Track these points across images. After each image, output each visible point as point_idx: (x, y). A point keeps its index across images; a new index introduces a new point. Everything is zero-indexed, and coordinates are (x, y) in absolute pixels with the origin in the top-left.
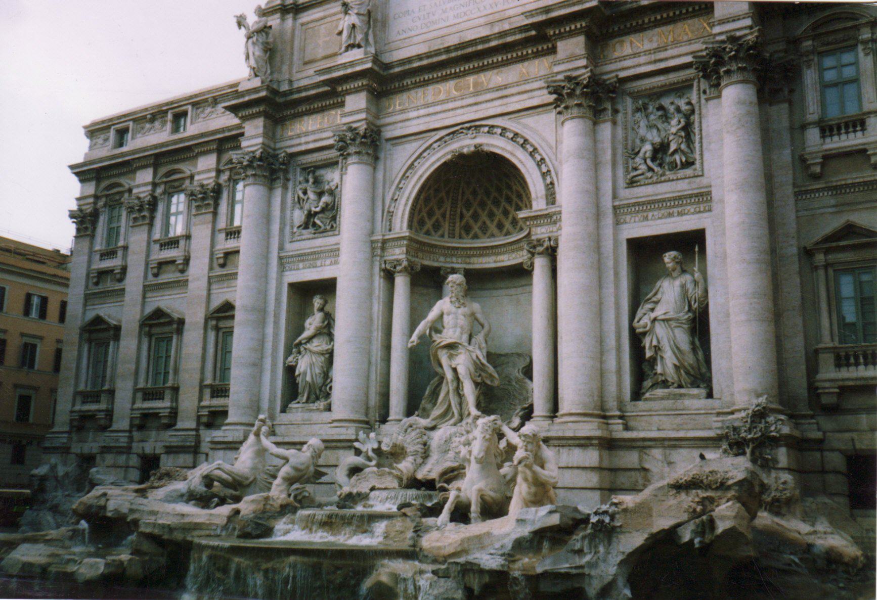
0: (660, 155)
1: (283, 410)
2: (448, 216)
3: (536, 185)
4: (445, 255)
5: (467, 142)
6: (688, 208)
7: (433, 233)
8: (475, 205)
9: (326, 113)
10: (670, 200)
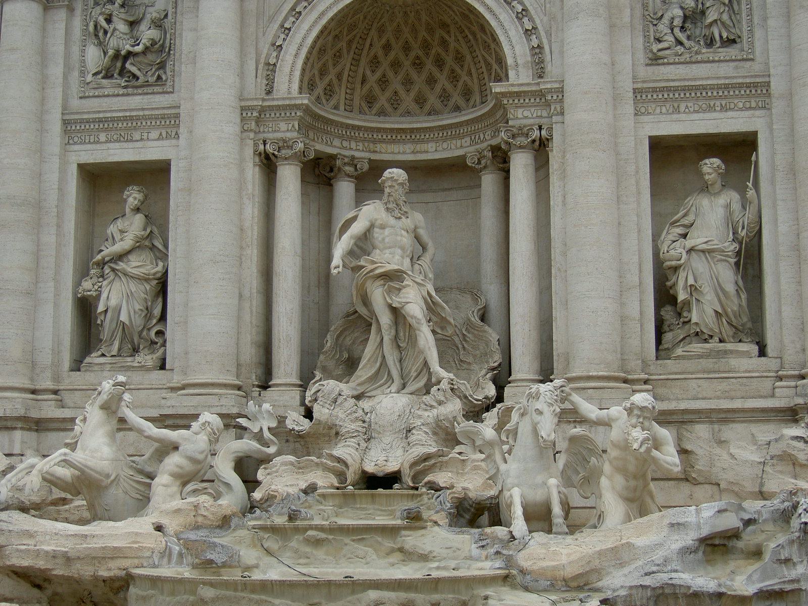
0: (688, 25)
1: (77, 365)
3: (514, 47)
4: (342, 137)
6: (736, 102)
7: (324, 101)
8: (385, 65)
10: (712, 87)
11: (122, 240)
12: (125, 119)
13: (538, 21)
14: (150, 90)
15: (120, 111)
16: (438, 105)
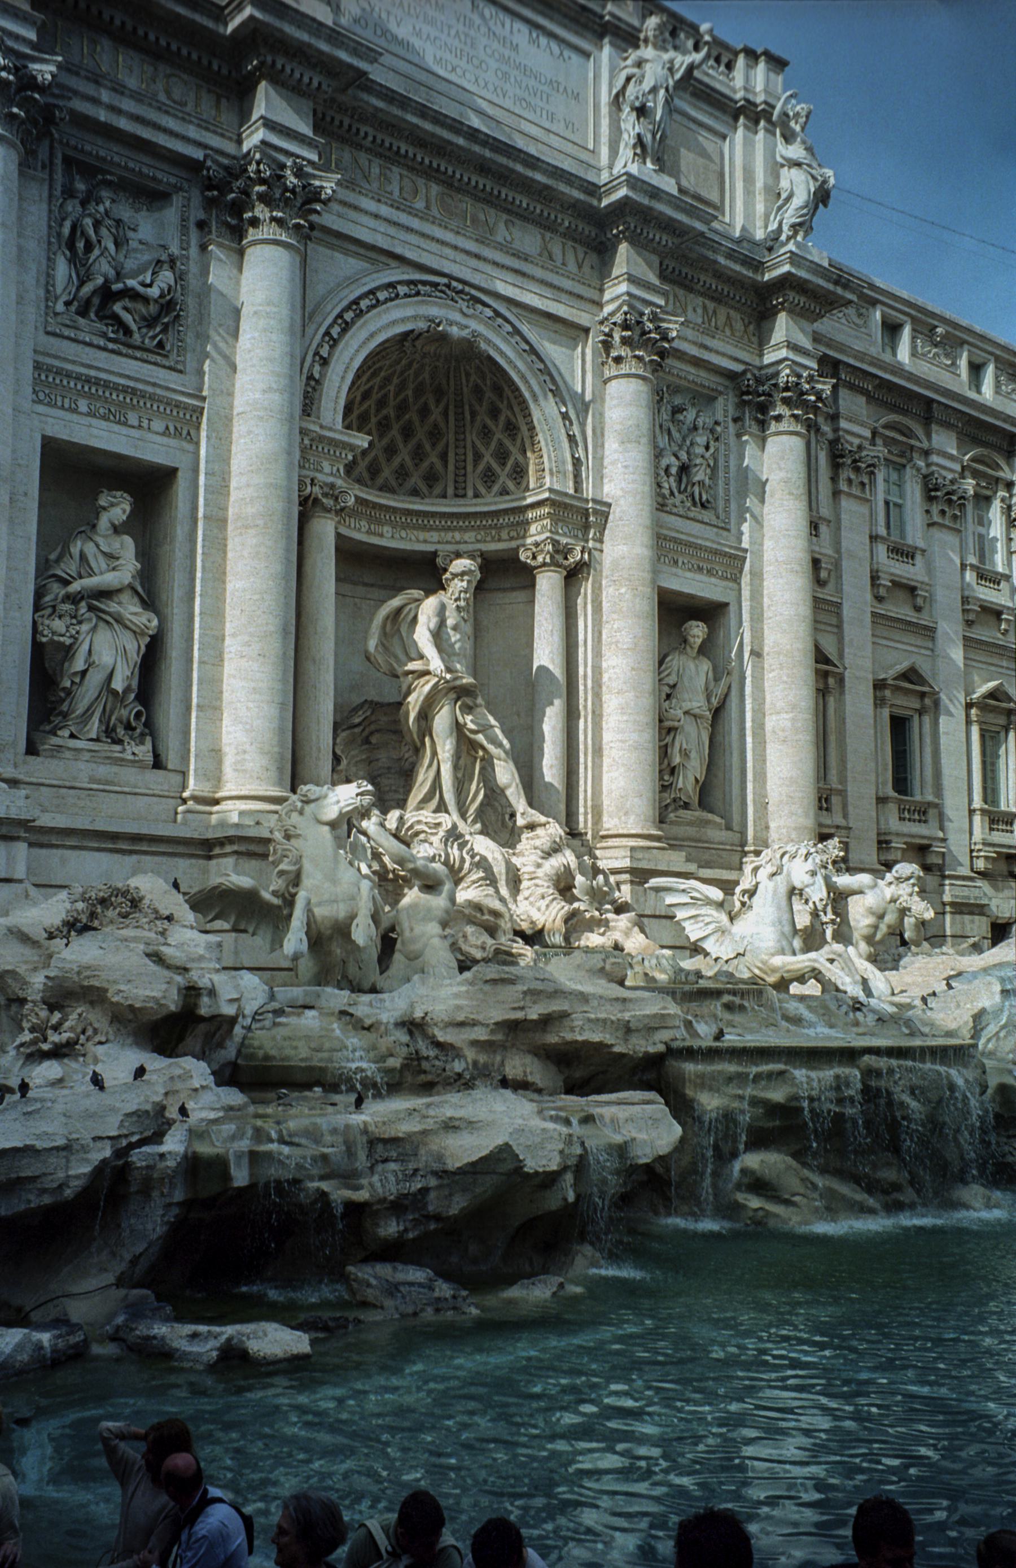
1: (32, 750)
5: (457, 317)
8: (356, 413)
10: (706, 549)
12: (125, 390)
14: (152, 358)
15: (121, 375)
16: (394, 483)
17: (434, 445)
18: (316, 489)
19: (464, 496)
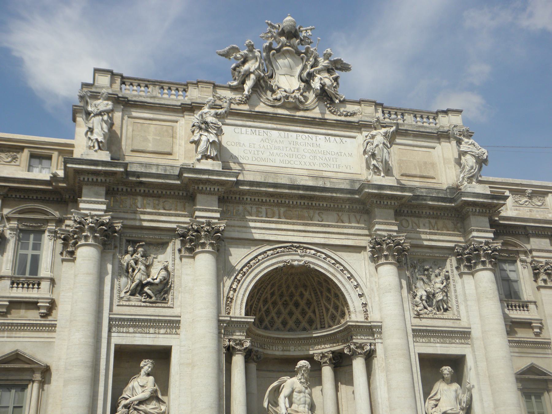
2: (253, 308)
5: (298, 257)
8: (270, 303)
9: (162, 200)
10: (446, 332)
11: (143, 392)
12: (147, 320)
13: (364, 291)
14: (160, 305)
16: (294, 327)
17: (309, 308)
18: (231, 343)
19: (324, 328)
